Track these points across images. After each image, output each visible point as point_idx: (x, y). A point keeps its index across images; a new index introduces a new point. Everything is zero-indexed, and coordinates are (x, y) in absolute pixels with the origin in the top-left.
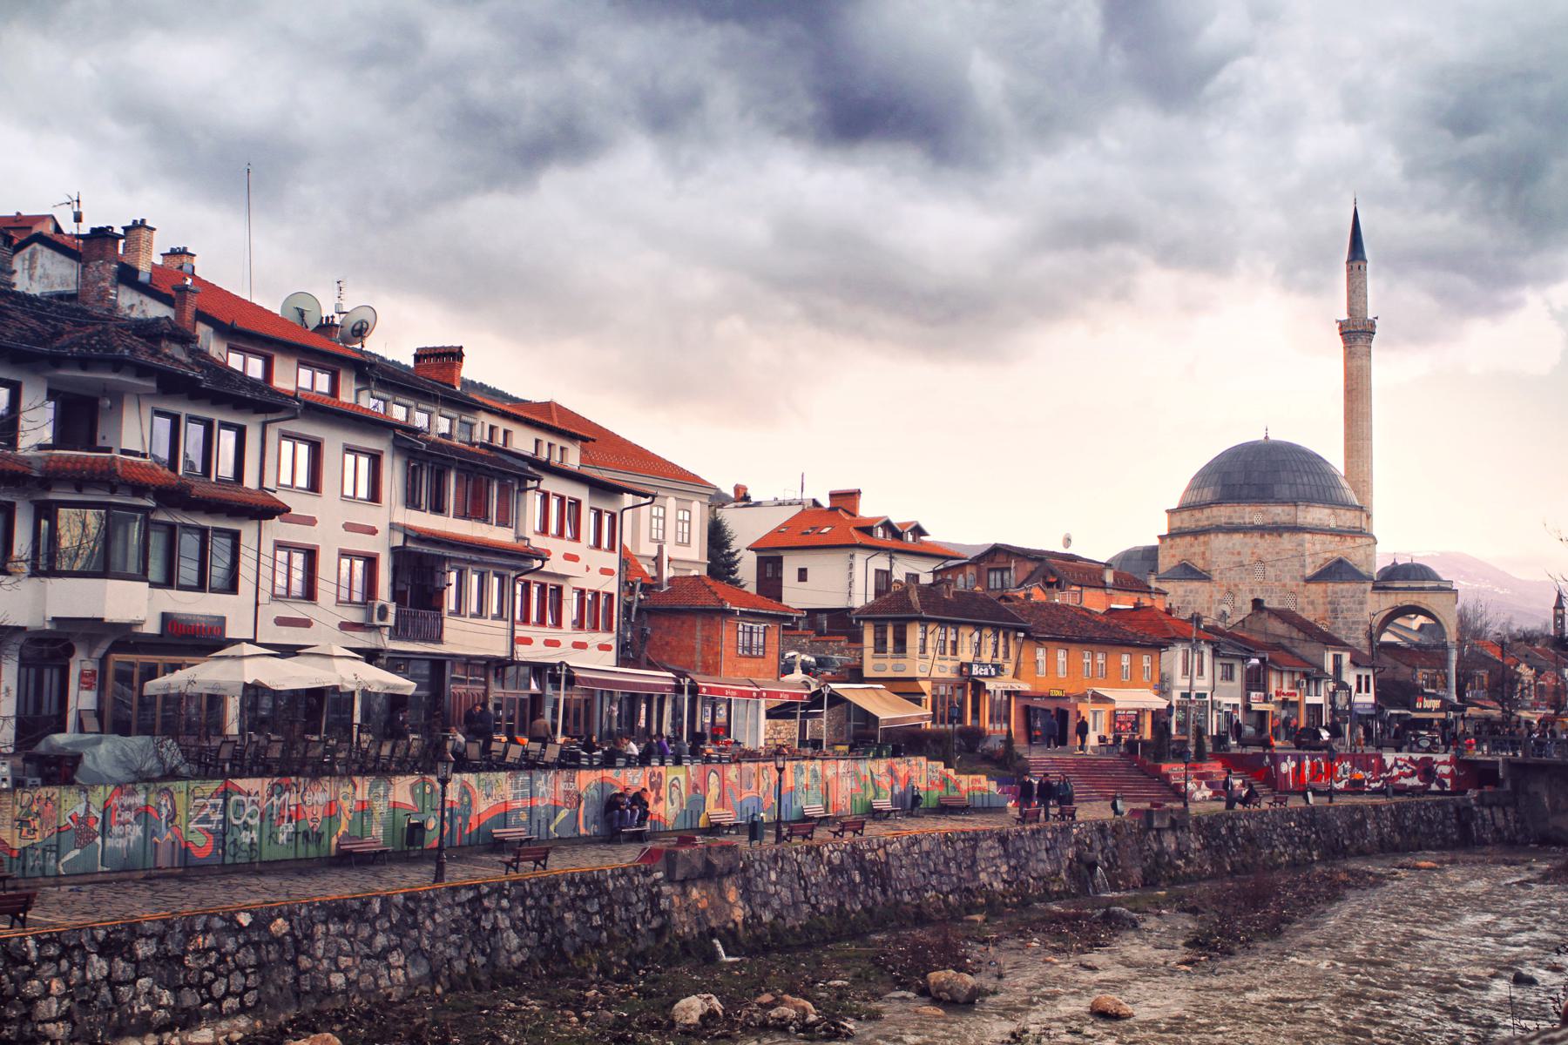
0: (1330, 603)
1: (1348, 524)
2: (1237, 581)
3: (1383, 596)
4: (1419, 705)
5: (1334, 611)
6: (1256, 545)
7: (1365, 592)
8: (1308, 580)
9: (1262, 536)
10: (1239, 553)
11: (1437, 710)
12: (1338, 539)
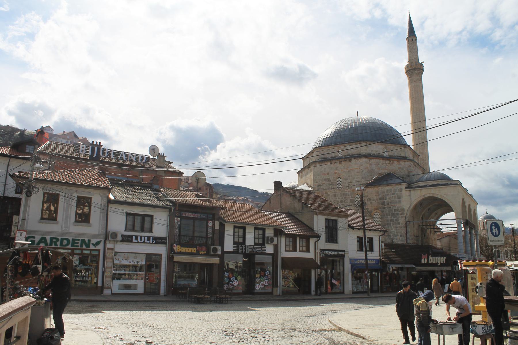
0: (380, 199)
1: (396, 154)
2: (327, 191)
3: (412, 192)
4: (424, 261)
5: (383, 204)
6: (337, 168)
7: (401, 190)
8: (367, 186)
9: (340, 162)
10: (328, 174)
11: (442, 265)
12: (388, 162)
